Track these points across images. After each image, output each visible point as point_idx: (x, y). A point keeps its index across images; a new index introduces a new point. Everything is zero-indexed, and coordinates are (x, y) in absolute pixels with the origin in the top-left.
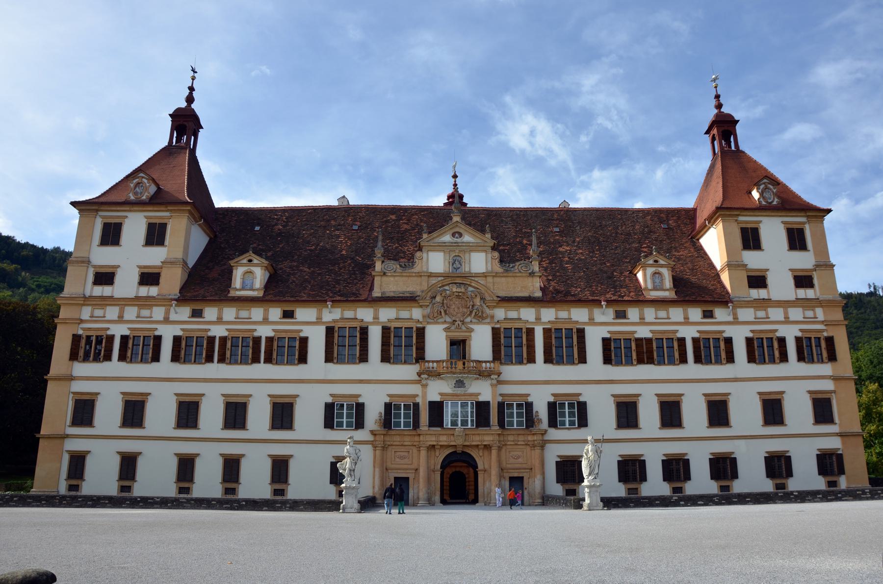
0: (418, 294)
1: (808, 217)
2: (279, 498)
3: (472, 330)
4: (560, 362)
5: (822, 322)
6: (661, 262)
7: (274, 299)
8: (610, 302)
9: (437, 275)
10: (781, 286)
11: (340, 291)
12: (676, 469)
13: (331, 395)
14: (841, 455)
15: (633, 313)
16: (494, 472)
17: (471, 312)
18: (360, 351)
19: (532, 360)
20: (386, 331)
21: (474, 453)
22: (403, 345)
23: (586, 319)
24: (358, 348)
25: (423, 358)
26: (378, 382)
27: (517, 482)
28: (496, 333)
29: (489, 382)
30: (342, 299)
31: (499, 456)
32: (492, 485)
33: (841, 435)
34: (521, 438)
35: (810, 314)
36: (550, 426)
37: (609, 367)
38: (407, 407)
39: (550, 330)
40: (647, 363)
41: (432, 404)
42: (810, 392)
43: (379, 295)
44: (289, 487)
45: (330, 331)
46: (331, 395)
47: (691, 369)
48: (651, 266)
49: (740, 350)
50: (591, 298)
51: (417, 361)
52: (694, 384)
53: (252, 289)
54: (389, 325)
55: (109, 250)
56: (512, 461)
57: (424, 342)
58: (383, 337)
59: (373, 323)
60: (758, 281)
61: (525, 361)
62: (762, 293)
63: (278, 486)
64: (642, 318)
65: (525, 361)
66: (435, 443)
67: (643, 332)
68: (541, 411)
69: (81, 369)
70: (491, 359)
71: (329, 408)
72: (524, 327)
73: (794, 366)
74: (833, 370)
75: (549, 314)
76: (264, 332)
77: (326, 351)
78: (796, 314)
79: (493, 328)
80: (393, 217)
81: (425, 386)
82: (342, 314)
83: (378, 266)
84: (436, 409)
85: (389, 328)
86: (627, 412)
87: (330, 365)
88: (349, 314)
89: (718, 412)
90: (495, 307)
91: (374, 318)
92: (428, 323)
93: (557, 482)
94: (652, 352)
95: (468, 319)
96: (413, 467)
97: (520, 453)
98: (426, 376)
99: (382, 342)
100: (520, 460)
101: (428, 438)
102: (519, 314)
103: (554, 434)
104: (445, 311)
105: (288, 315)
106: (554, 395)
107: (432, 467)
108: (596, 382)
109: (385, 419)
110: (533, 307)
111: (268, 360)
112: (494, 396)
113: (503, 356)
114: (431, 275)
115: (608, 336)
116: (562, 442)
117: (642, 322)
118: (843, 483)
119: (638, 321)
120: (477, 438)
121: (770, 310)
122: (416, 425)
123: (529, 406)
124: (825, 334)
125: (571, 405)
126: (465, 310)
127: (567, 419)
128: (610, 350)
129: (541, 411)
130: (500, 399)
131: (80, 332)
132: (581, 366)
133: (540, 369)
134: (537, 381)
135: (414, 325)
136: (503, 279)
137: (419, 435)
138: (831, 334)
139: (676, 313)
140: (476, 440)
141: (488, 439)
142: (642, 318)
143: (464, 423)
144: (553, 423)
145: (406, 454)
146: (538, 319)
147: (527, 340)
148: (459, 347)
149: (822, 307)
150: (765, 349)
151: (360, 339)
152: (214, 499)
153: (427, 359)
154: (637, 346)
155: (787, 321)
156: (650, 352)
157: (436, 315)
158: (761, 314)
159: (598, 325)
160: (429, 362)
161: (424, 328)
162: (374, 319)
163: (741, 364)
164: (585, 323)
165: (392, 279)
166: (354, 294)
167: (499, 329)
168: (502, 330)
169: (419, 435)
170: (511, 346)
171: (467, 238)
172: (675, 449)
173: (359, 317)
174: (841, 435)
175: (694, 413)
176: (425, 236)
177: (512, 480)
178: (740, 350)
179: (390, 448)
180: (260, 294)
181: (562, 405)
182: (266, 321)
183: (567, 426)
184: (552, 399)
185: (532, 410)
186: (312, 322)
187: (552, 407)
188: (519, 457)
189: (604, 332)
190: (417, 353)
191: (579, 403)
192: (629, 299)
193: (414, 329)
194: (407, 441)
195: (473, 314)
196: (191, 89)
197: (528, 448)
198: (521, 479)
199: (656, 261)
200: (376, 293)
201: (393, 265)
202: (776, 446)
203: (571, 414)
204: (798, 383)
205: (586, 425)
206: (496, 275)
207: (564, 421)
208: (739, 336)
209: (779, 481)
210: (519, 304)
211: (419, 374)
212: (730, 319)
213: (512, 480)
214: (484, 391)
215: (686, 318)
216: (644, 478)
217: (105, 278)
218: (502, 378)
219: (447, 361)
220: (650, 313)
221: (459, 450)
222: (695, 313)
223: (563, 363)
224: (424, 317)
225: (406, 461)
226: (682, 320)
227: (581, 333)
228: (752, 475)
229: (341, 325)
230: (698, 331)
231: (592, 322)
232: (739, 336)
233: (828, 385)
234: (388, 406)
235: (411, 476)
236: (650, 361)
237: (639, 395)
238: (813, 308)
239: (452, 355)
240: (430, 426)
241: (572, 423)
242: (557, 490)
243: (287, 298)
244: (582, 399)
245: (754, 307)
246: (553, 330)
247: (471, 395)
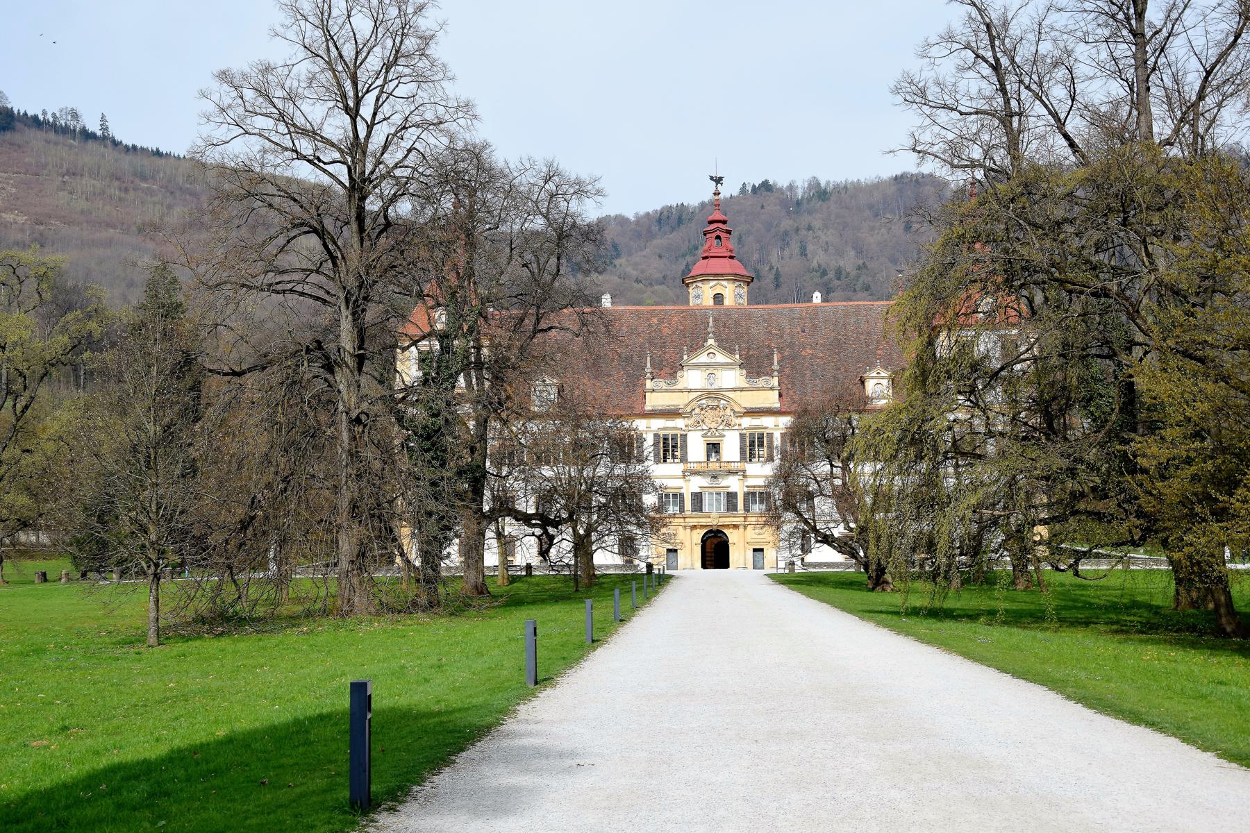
9: (696, 391)
20: (656, 436)
28: (742, 436)
38: (675, 495)
80: (655, 320)
83: (649, 384)
114: (690, 391)
122: (682, 510)
135: (679, 433)
140: (727, 521)
171: (721, 358)
176: (685, 357)
177: (755, 550)
200: (648, 407)
201: (661, 384)
206: (742, 390)
211: (684, 472)
214: (734, 484)
239: (708, 457)
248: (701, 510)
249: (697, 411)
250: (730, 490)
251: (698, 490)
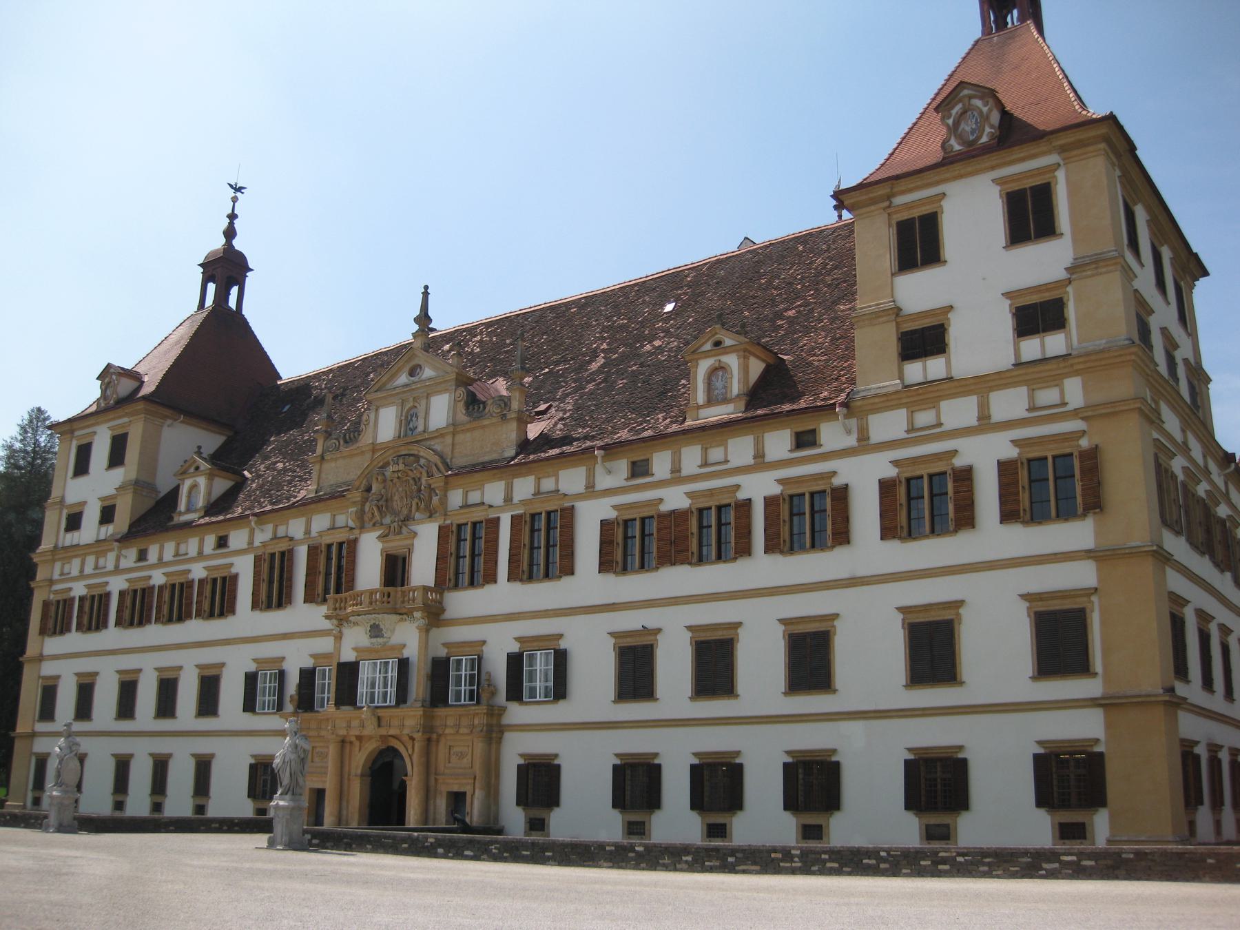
1: (1062, 150)
5: (1075, 413)
6: (728, 342)
8: (612, 450)
10: (982, 339)
12: (718, 785)
13: (255, 660)
14: (1101, 755)
20: (313, 551)
22: (333, 574)
33: (1107, 704)
35: (1048, 396)
36: (508, 700)
37: (610, 578)
42: (1026, 597)
45: (258, 561)
46: (255, 660)
47: (762, 568)
48: (707, 355)
49: (866, 512)
52: (757, 596)
55: (82, 480)
60: (925, 339)
62: (935, 367)
63: (200, 801)
67: (675, 499)
68: (498, 670)
69: (53, 645)
73: (992, 536)
74: (1097, 534)
75: (524, 487)
76: (198, 572)
78: (1009, 403)
81: (339, 638)
84: (348, 673)
86: (635, 671)
87: (257, 613)
89: (810, 658)
103: (517, 713)
106: (519, 639)
108: (587, 609)
110: (501, 479)
112: (425, 645)
116: (531, 730)
117: (677, 477)
118: (1101, 825)
121: (944, 405)
124: (1084, 443)
130: (442, 653)
131: (52, 596)
132: (566, 580)
133: (503, 594)
134: (496, 615)
136: (468, 435)
138: (1097, 440)
139: (740, 449)
144: (515, 692)
149: (1077, 373)
150: (927, 502)
155: (985, 424)
158: (924, 418)
159: (596, 498)
161: (356, 541)
163: (868, 547)
164: (579, 497)
165: (333, 464)
172: (716, 741)
174: (1107, 704)
175: (761, 663)
178: (866, 512)
187: (515, 662)
196: (232, 217)
199: (718, 344)
202: (935, 735)
204: (997, 577)
208: (864, 477)
209: (935, 819)
210: (478, 476)
212: (851, 441)
215: (759, 455)
217: (74, 522)
220: (691, 457)
222: (779, 443)
226: (751, 461)
227: (569, 514)
228: (874, 803)
230: (780, 481)
231: (591, 491)
232: (864, 477)
233: (1083, 575)
238: (1056, 380)
245: (906, 405)
247: (393, 648)
250: (406, 653)
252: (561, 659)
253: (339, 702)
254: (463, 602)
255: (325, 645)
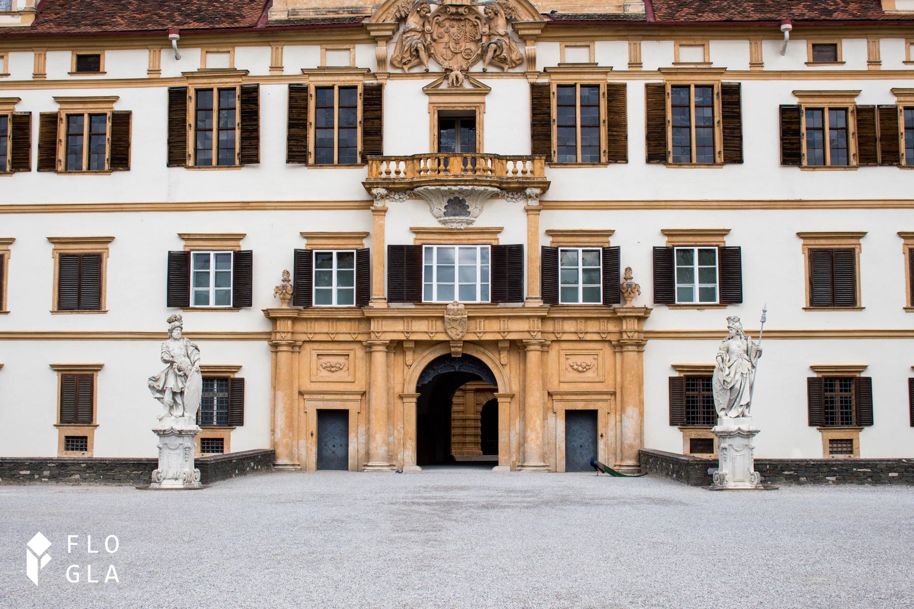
0: (368, 12)
2: (77, 455)
3: (484, 91)
4: (683, 159)
7: (55, 30)
8: (801, 28)
11: (199, 10)
15: (854, 52)
16: (536, 397)
17: (484, 52)
18: (243, 139)
19: (618, 154)
20: (297, 94)
21: (488, 359)
22: (335, 125)
23: (744, 65)
24: (238, 132)
25: (379, 152)
26: (281, 206)
27: (582, 420)
28: (539, 95)
29: (521, 204)
30: (201, 26)
31: (543, 363)
32: (531, 427)
34: (593, 326)
39: (661, 88)
40: (883, 164)
41: (394, 251)
43: (283, 16)
44: (97, 431)
45: (177, 98)
50: (756, 16)
51: (365, 161)
53: (10, 13)
54: (304, 81)
56: (572, 375)
57: (380, 118)
58: (291, 108)
59: (268, 79)
61: (604, 159)
64: (874, 62)
65: (604, 159)
66: (402, 337)
67: (876, 94)
68: (638, 268)
70: (526, 150)
71: (178, 265)
72: (603, 81)
75: (659, 55)
76: (37, 103)
77: (170, 142)
79: (534, 87)
82: (204, 61)
85: (305, 89)
88: (217, 61)
90: (536, 39)
91: (272, 68)
92: (390, 76)
93: (672, 423)
94: (895, 138)
95: (478, 68)
96: (359, 387)
97: (589, 360)
98: (383, 191)
99: (290, 119)
100: (590, 375)
101: (387, 326)
102: (592, 54)
103: (664, 318)
104: (427, 49)
105: (88, 64)
106: (667, 233)
107: (398, 389)
108: (763, 203)
109: (296, 287)
111: (48, 164)
112: (532, 232)
113: (554, 147)
115: (794, 101)
117: (875, 70)
119: (864, 67)
120: (495, 326)
122: (364, 296)
123: (611, 256)
125: (707, 256)
126: (472, 46)
127: (697, 286)
128: (798, 133)
129: (638, 268)
130: (547, 242)
133: (636, 176)
134: (629, 203)
135: (360, 82)
137: (369, 319)
140: (490, 330)
141: (517, 329)
142: (874, 62)
143: (467, 291)
145: (341, 360)
146: (635, 63)
147: (610, 111)
148: (457, 126)
151: (243, 112)
152: (51, 460)
153: (388, 151)
154: (860, 124)
156: (891, 138)
157: (407, 56)
159: (770, 77)
160: (389, 159)
161: (379, 89)
162: (273, 71)
166: (228, 16)
167: (547, 87)
168: (554, 89)
169: (369, 319)
170: (574, 124)
173: (239, 67)
177: (571, 415)
179: (308, 347)
180: (28, 21)
181: (686, 255)
182: (39, 80)
183: (697, 301)
184: (663, 242)
185: (617, 265)
186: (138, 83)
187: (663, 260)
188: (587, 368)
189: (783, 93)
190: (365, 142)
191: (724, 251)
192: (846, 17)
193: (360, 90)
194: (344, 330)
195: (490, 54)
197: (607, 350)
198: (592, 415)
203: (706, 276)
205: (738, 300)
207: (691, 290)
211: (368, 186)
213: (571, 415)
214: (510, 222)
216: (865, 418)
218: (551, 195)
219: (426, 157)
221: (457, 351)
223: (690, 163)
224: (381, 62)
225: (341, 375)
227: (732, 95)
229: (202, 83)
231: (757, 70)
234: (302, 259)
235: (353, 407)
236: (891, 158)
237: (860, 235)
239: (442, 147)
240: (392, 298)
241: (707, 295)
242: (673, 441)
243: (83, 29)
244: (730, 242)
246: (669, 89)
248: (414, 295)
249: (413, 22)
250: (504, 240)
251: (409, 240)
252: (731, 261)
253: (393, 296)
254: (569, 181)
255: (350, 222)
